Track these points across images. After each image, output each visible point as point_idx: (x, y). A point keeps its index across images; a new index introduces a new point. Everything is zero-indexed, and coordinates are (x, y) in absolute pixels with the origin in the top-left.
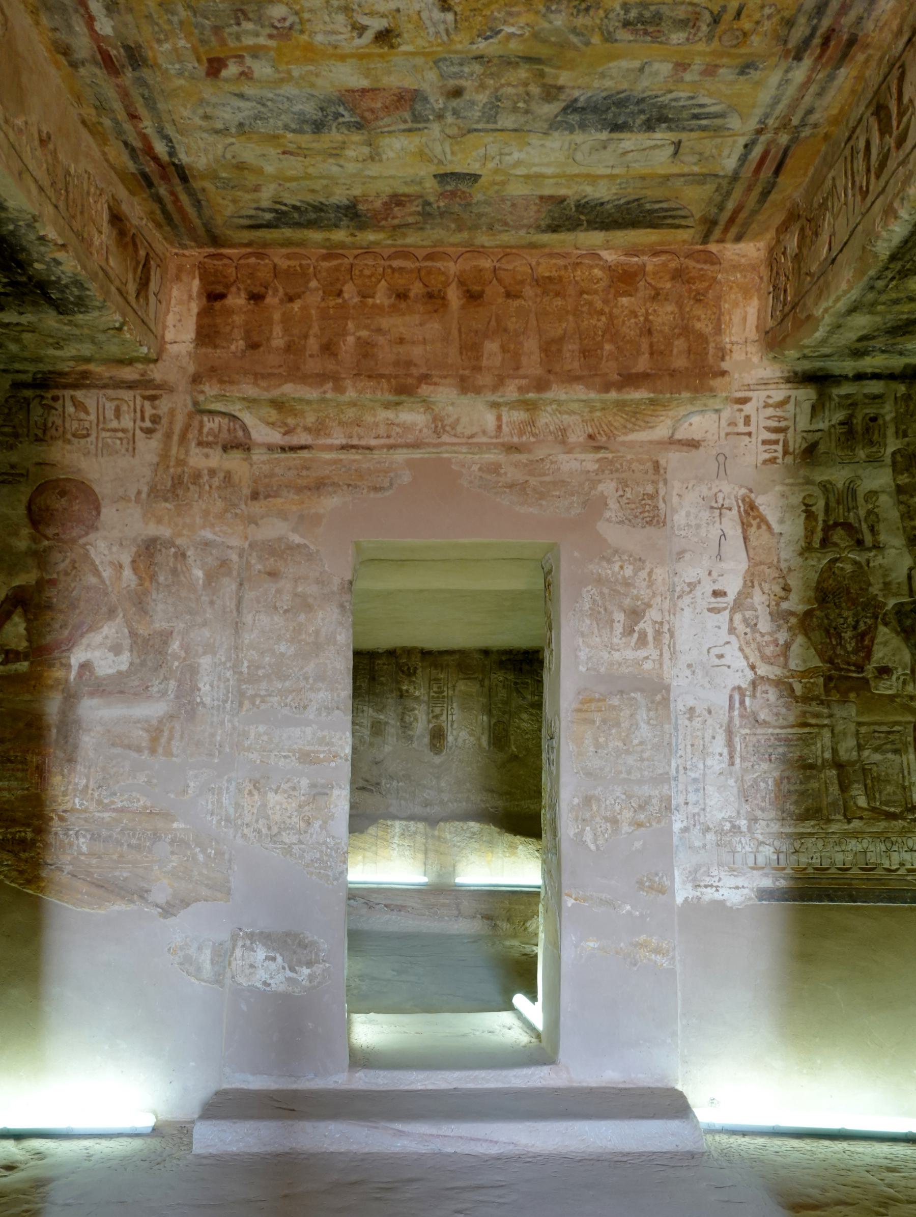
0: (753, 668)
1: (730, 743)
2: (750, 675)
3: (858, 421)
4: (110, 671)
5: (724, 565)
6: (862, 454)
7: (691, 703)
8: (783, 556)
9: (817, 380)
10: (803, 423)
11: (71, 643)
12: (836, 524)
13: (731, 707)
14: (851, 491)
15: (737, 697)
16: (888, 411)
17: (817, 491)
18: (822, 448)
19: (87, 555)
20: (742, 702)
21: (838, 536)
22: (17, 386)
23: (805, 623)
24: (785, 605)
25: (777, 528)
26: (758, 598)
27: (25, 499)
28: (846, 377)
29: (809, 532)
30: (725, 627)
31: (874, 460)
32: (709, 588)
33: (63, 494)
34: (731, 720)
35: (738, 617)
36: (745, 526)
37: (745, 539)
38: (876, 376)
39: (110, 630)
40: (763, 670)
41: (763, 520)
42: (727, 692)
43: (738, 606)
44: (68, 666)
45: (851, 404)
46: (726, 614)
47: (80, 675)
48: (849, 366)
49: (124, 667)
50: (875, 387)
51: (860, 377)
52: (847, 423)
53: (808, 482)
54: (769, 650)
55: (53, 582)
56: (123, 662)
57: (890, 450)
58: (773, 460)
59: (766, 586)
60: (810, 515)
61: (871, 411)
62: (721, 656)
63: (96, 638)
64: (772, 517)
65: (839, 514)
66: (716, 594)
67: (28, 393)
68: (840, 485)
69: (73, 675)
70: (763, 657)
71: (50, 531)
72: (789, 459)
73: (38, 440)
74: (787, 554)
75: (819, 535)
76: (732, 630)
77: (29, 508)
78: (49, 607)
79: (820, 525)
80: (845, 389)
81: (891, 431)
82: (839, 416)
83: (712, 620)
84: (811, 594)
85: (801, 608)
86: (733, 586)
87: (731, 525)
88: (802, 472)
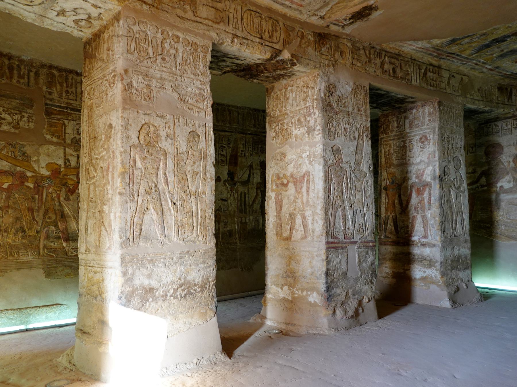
4: (508, 187)
11: (497, 182)
19: (500, 160)
22: (480, 124)
27: (484, 150)
33: (493, 147)
39: (507, 178)
44: (497, 187)
47: (500, 189)
49: (512, 186)
55: (492, 168)
56: (511, 185)
63: (504, 180)
67: (483, 126)
69: (498, 189)
71: (491, 156)
73: (486, 136)
77: (485, 152)
78: (491, 174)
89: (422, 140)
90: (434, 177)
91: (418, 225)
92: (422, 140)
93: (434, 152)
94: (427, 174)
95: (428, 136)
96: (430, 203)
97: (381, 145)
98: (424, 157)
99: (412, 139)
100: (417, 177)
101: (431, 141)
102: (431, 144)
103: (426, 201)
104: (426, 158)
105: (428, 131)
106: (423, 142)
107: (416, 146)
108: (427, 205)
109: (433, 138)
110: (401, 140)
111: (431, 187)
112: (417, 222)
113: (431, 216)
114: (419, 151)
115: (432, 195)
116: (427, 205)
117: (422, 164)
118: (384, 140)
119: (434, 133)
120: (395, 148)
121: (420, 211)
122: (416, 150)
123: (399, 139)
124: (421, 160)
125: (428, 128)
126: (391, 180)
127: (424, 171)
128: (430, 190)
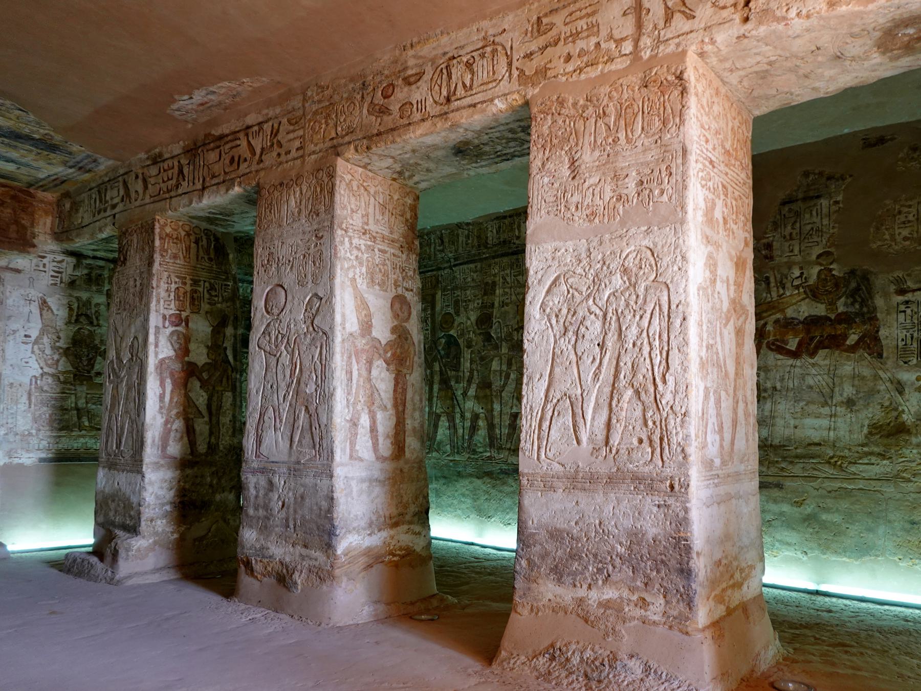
0: (42, 368)
1: (29, 399)
2: (40, 371)
3: (93, 275)
5: (30, 325)
6: (94, 288)
7: (11, 381)
8: (58, 324)
9: (78, 255)
10: (70, 271)
12: (82, 314)
13: (31, 384)
14: (89, 302)
15: (34, 380)
16: (106, 274)
17: (74, 300)
18: (77, 282)
20: (36, 382)
21: (82, 319)
23: (66, 352)
24: (57, 344)
25: (56, 312)
26: (46, 340)
28: (89, 257)
29: (70, 316)
30: (30, 351)
31: (99, 292)
32: (23, 333)
34: (30, 390)
35: (36, 347)
36: (41, 310)
37: (41, 315)
38: (101, 259)
40: (46, 370)
41: (49, 308)
42: (29, 378)
43: (36, 342)
45: (90, 267)
46: (30, 345)
48: (90, 253)
50: (101, 263)
51: (95, 258)
52: (88, 275)
53: (71, 295)
54: (50, 362)
57: (106, 288)
58: (55, 284)
59: (50, 336)
60: (71, 309)
61: (99, 272)
62: (27, 363)
64: (54, 308)
65: (84, 310)
66: (26, 336)
68: (84, 299)
70: (47, 365)
72: (63, 285)
74: (60, 324)
75: (74, 318)
76: (33, 352)
79: (75, 314)
80: (88, 261)
81: (106, 282)
82: (85, 271)
83: (24, 347)
84: (70, 341)
85: (65, 346)
86: (34, 334)
87: (36, 311)
88: (68, 291)
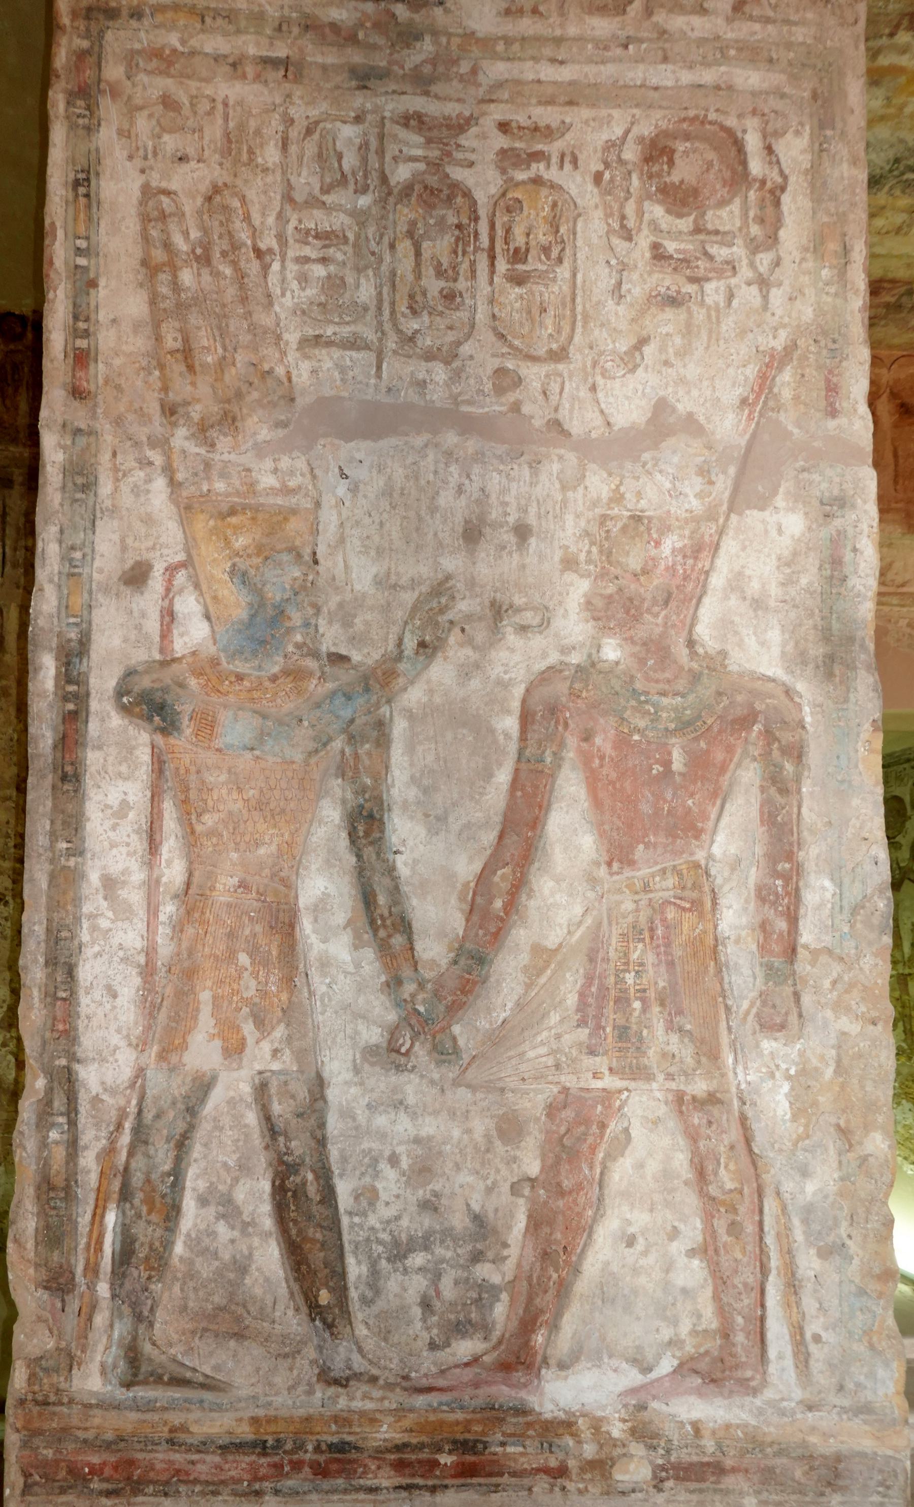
89: (684, 171)
90: (826, 635)
91: (640, 1219)
92: (684, 171)
93: (827, 335)
94: (737, 583)
95: (753, 142)
96: (782, 949)
97: (86, 94)
98: (713, 387)
99: (548, 133)
100: (616, 609)
101: (795, 204)
102: (793, 234)
103: (734, 916)
104: (731, 395)
105: (750, 78)
106: (680, 199)
107: (592, 228)
108: (744, 974)
109: (815, 174)
110: (392, 106)
111: (797, 753)
112: (621, 1172)
113: (802, 1109)
114: (636, 289)
115: (812, 853)
116: (744, 974)
117: (678, 453)
118: (144, 36)
119: (824, 111)
120: (306, 180)
121: (660, 1038)
122: (600, 278)
123: (364, 79)
124: (661, 407)
125: (752, 54)
126: (236, 602)
127: (702, 550)
128: (779, 787)
